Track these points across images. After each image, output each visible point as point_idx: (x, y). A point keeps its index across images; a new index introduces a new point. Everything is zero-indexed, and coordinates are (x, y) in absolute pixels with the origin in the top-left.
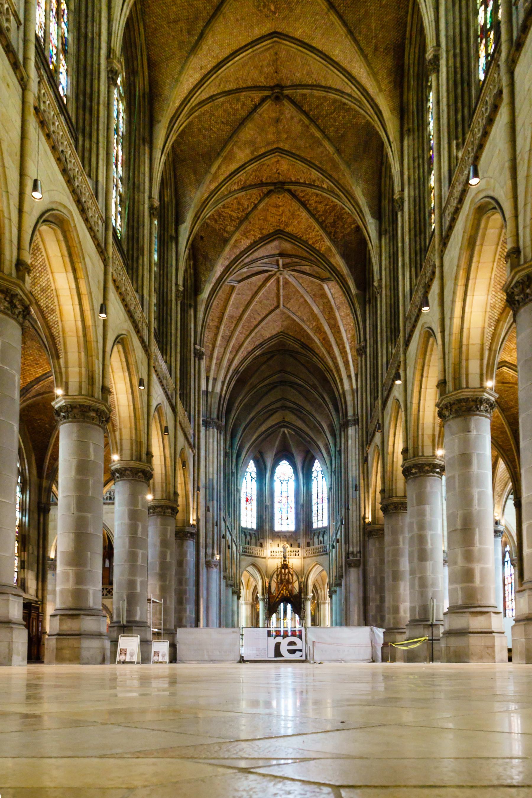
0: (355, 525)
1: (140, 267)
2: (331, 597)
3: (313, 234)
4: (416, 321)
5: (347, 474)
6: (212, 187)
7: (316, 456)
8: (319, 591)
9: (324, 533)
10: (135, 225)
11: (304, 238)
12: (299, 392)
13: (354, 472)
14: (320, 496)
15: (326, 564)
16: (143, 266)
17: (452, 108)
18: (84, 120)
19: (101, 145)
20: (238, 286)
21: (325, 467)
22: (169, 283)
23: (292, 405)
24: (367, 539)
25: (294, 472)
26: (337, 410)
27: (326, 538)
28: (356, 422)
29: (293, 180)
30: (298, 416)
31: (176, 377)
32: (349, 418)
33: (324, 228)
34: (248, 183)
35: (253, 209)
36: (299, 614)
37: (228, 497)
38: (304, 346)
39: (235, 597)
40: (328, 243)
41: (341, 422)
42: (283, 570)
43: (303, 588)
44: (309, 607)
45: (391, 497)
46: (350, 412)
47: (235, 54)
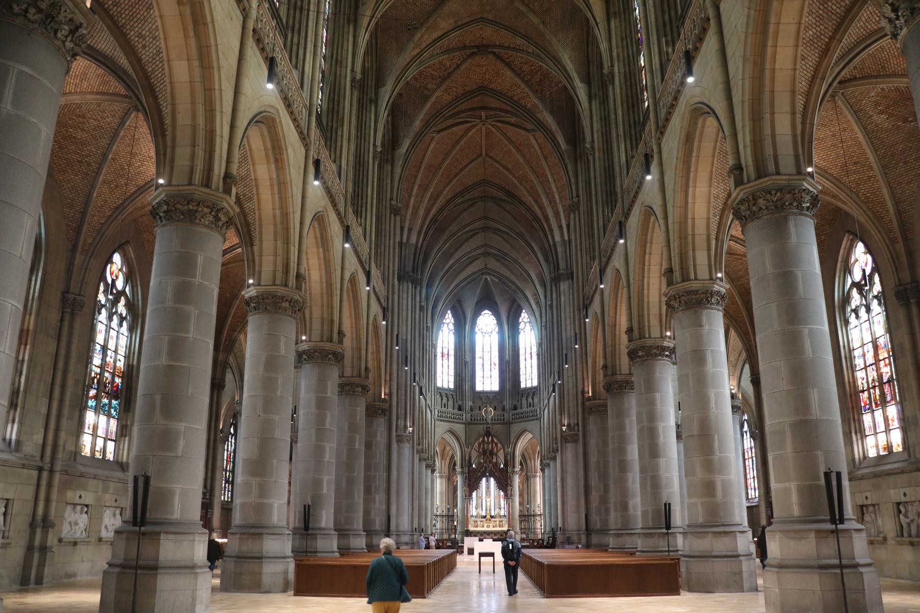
0: (571, 391)
1: (339, 138)
2: (542, 470)
3: (519, 91)
4: (635, 197)
5: (560, 333)
6: (415, 53)
7: (522, 304)
8: (528, 462)
9: (534, 394)
10: (336, 98)
11: (509, 94)
12: (503, 238)
13: (568, 332)
14: (528, 351)
15: (537, 431)
16: (342, 136)
17: (659, 9)
18: (294, 18)
19: (309, 39)
20: (437, 136)
21: (533, 319)
22: (367, 144)
23: (496, 252)
24: (587, 415)
25: (497, 323)
26: (547, 260)
27: (536, 400)
28: (570, 276)
29: (498, 43)
31: (371, 240)
32: (561, 272)
33: (530, 87)
34: (451, 46)
35: (455, 70)
36: (505, 491)
37: (420, 357)
38: (509, 194)
39: (429, 471)
40: (536, 101)
41: (553, 275)
43: (509, 461)
44: (517, 481)
45: (614, 374)
46: (562, 266)
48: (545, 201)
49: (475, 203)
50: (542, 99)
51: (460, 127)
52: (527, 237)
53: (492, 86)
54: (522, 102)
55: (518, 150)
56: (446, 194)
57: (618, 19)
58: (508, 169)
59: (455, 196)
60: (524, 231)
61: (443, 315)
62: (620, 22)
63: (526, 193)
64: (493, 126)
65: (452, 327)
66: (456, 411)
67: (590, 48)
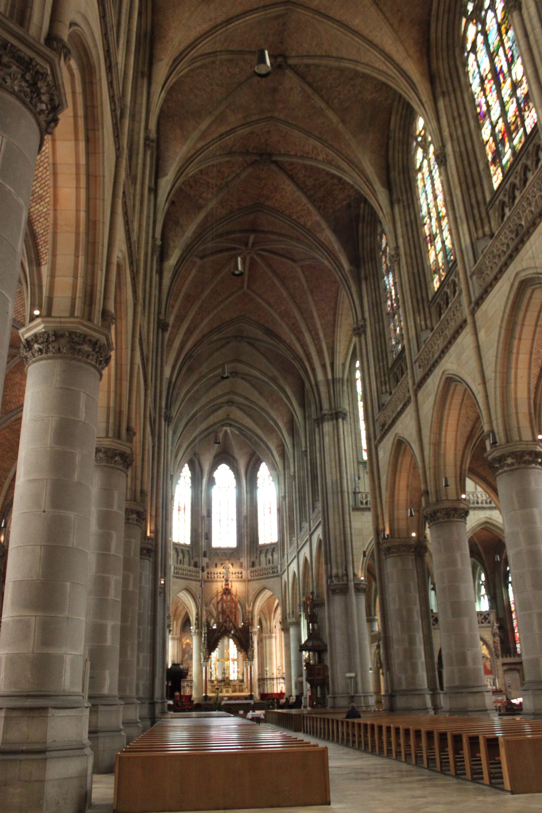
30: (245, 413)
42: (225, 597)
47: (245, 13)
48: (308, 338)
49: (228, 343)
50: (323, 216)
51: (225, 254)
52: (282, 382)
53: (269, 203)
54: (302, 221)
55: (284, 284)
56: (204, 326)
57: (447, 99)
58: (269, 304)
59: (212, 332)
60: (277, 374)
61: (181, 467)
62: (450, 101)
63: (287, 330)
64: (259, 255)
65: (189, 481)
66: (192, 568)
67: (391, 153)
